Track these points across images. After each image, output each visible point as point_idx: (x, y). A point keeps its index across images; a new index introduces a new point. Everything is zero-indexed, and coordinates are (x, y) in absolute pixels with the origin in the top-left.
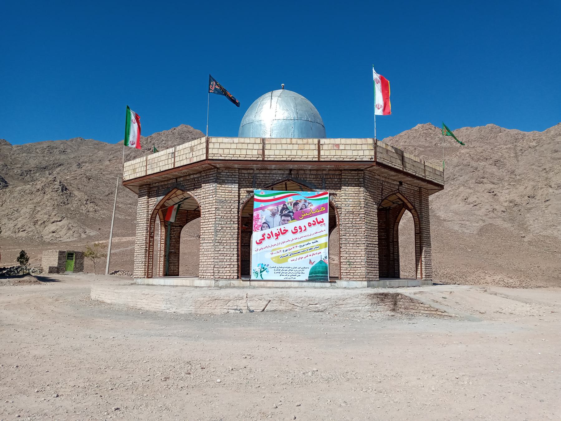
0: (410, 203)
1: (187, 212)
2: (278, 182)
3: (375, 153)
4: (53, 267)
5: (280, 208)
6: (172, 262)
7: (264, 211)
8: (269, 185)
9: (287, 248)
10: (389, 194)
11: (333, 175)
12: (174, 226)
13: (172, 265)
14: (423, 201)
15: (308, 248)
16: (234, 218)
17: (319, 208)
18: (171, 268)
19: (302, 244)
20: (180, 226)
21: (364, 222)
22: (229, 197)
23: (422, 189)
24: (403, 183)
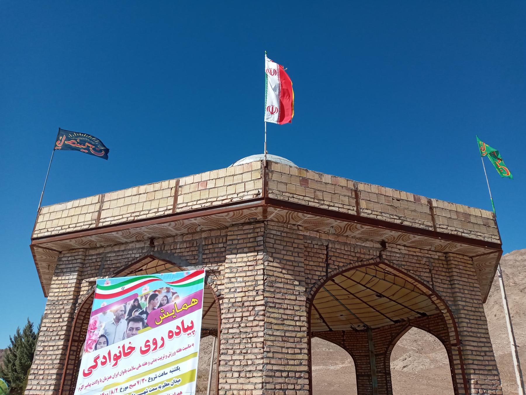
0: (423, 284)
2: (133, 262)
3: (266, 184)
5: (129, 307)
7: (105, 313)
8: (121, 268)
9: (128, 385)
10: (349, 267)
11: (216, 237)
14: (455, 278)
15: (162, 383)
16: (62, 330)
17: (188, 300)
19: (152, 376)
21: (262, 323)
22: (64, 294)
23: (451, 254)
24: (387, 244)
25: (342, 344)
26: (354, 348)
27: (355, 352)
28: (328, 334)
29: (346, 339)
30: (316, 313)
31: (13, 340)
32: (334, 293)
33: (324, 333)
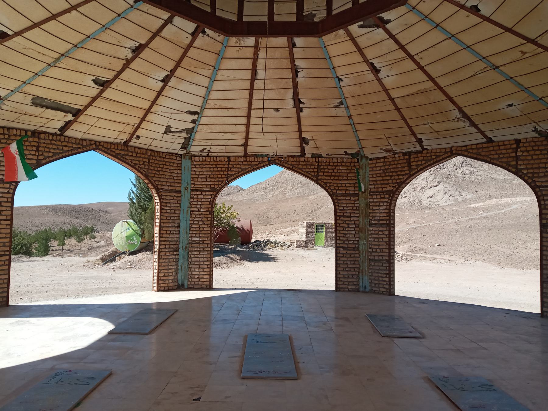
1: (229, 161)
4: (301, 241)
6: (195, 261)
12: (197, 191)
13: (194, 266)
18: (194, 273)
20: (213, 190)
25: (512, 166)
26: (538, 173)
27: (540, 180)
28: (483, 148)
29: (522, 155)
30: (451, 107)
31: (134, 183)
32: (485, 50)
33: (474, 147)
